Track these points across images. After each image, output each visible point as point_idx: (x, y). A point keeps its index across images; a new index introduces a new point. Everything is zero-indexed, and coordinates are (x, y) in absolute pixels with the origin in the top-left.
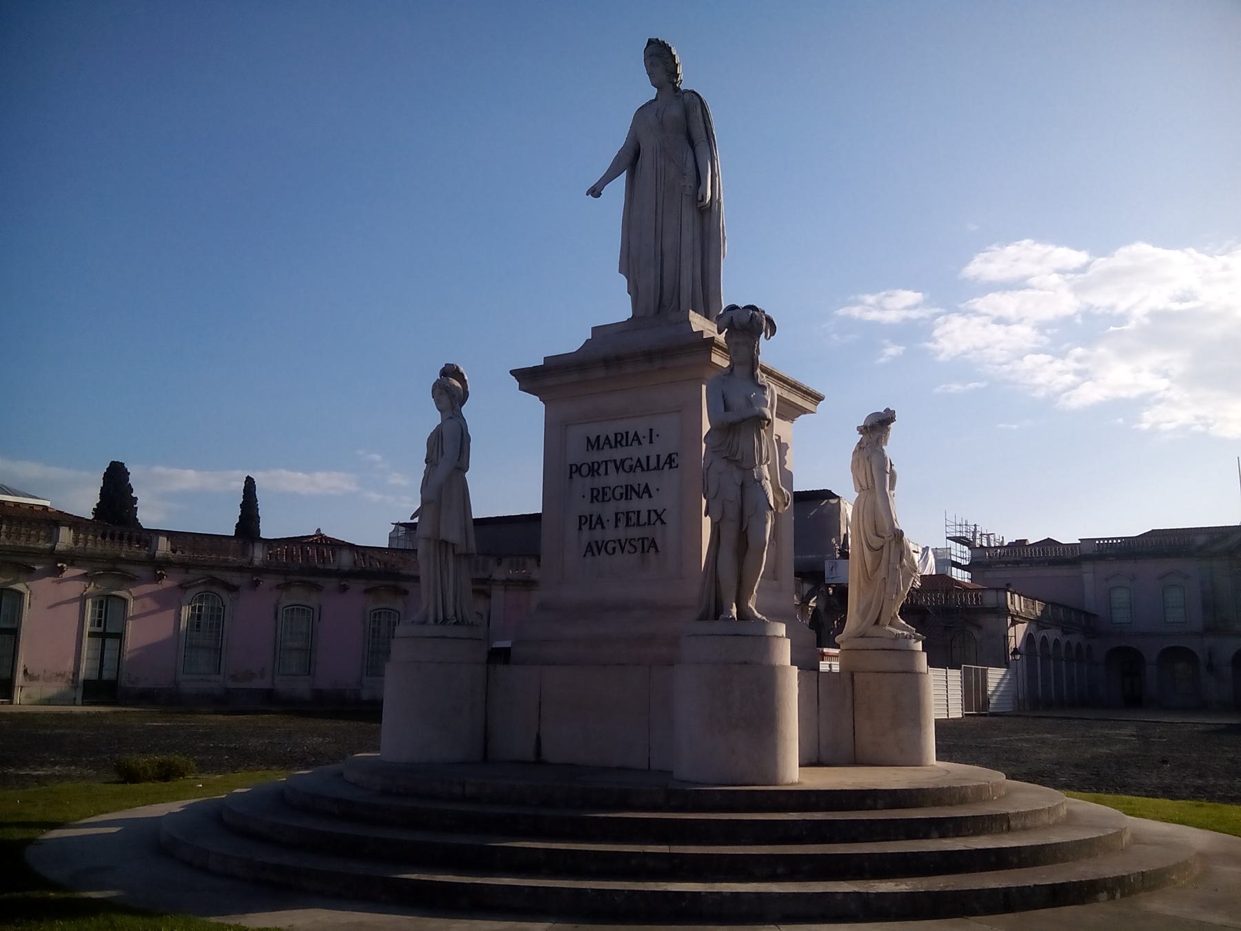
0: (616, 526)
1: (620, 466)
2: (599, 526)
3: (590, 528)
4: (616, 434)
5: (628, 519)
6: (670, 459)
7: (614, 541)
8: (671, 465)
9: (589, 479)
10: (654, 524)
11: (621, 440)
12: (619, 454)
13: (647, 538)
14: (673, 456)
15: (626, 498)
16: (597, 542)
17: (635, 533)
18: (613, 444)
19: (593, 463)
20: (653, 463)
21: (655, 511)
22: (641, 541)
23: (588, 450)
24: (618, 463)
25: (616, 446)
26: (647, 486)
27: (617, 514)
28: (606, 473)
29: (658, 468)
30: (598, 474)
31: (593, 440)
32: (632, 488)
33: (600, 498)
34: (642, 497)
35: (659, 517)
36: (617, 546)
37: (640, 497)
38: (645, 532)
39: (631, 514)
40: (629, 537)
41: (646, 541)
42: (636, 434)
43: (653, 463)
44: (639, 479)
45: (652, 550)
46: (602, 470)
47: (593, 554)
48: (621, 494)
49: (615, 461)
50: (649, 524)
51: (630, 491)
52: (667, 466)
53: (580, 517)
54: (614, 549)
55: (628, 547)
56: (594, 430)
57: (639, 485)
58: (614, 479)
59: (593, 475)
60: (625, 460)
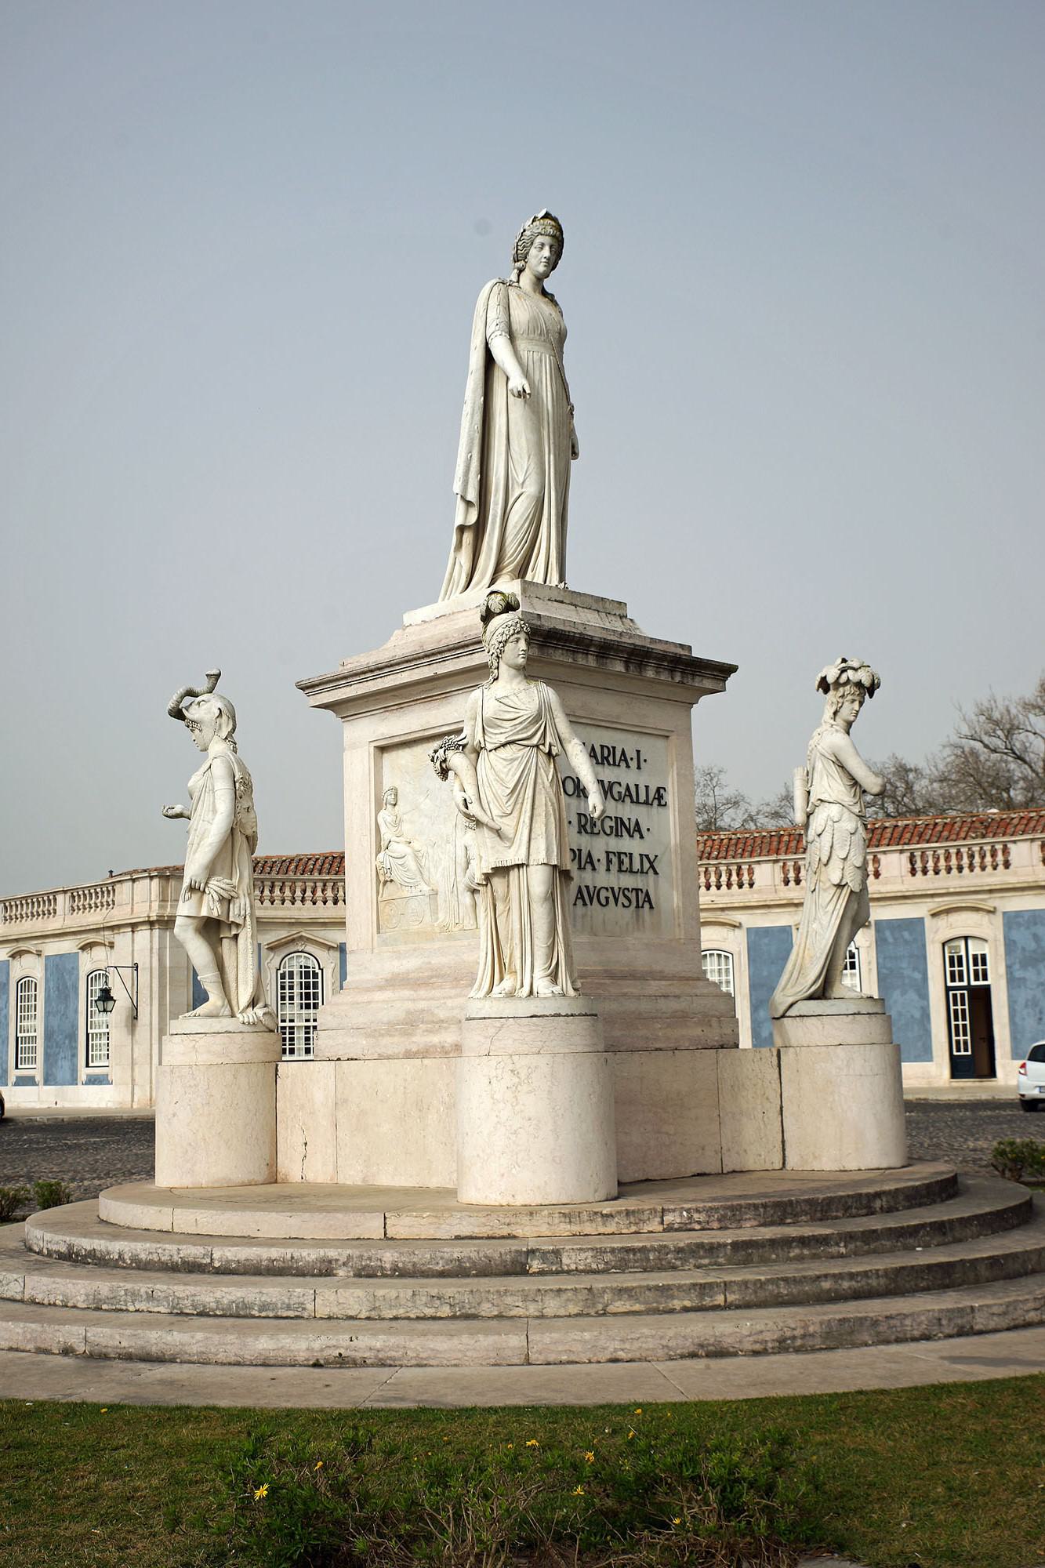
0: (608, 870)
2: (589, 866)
4: (602, 747)
5: (621, 862)
6: (659, 795)
7: (607, 889)
8: (659, 802)
13: (641, 890)
14: (662, 791)
15: (617, 835)
16: (587, 887)
17: (628, 881)
18: (600, 761)
21: (647, 856)
24: (606, 785)
26: (637, 823)
27: (608, 853)
29: (646, 803)
32: (623, 823)
36: (610, 894)
37: (631, 836)
39: (623, 857)
40: (623, 886)
43: (642, 798)
45: (647, 905)
47: (585, 904)
48: (611, 827)
52: (656, 802)
54: (607, 898)
55: (622, 899)
59: (579, 796)
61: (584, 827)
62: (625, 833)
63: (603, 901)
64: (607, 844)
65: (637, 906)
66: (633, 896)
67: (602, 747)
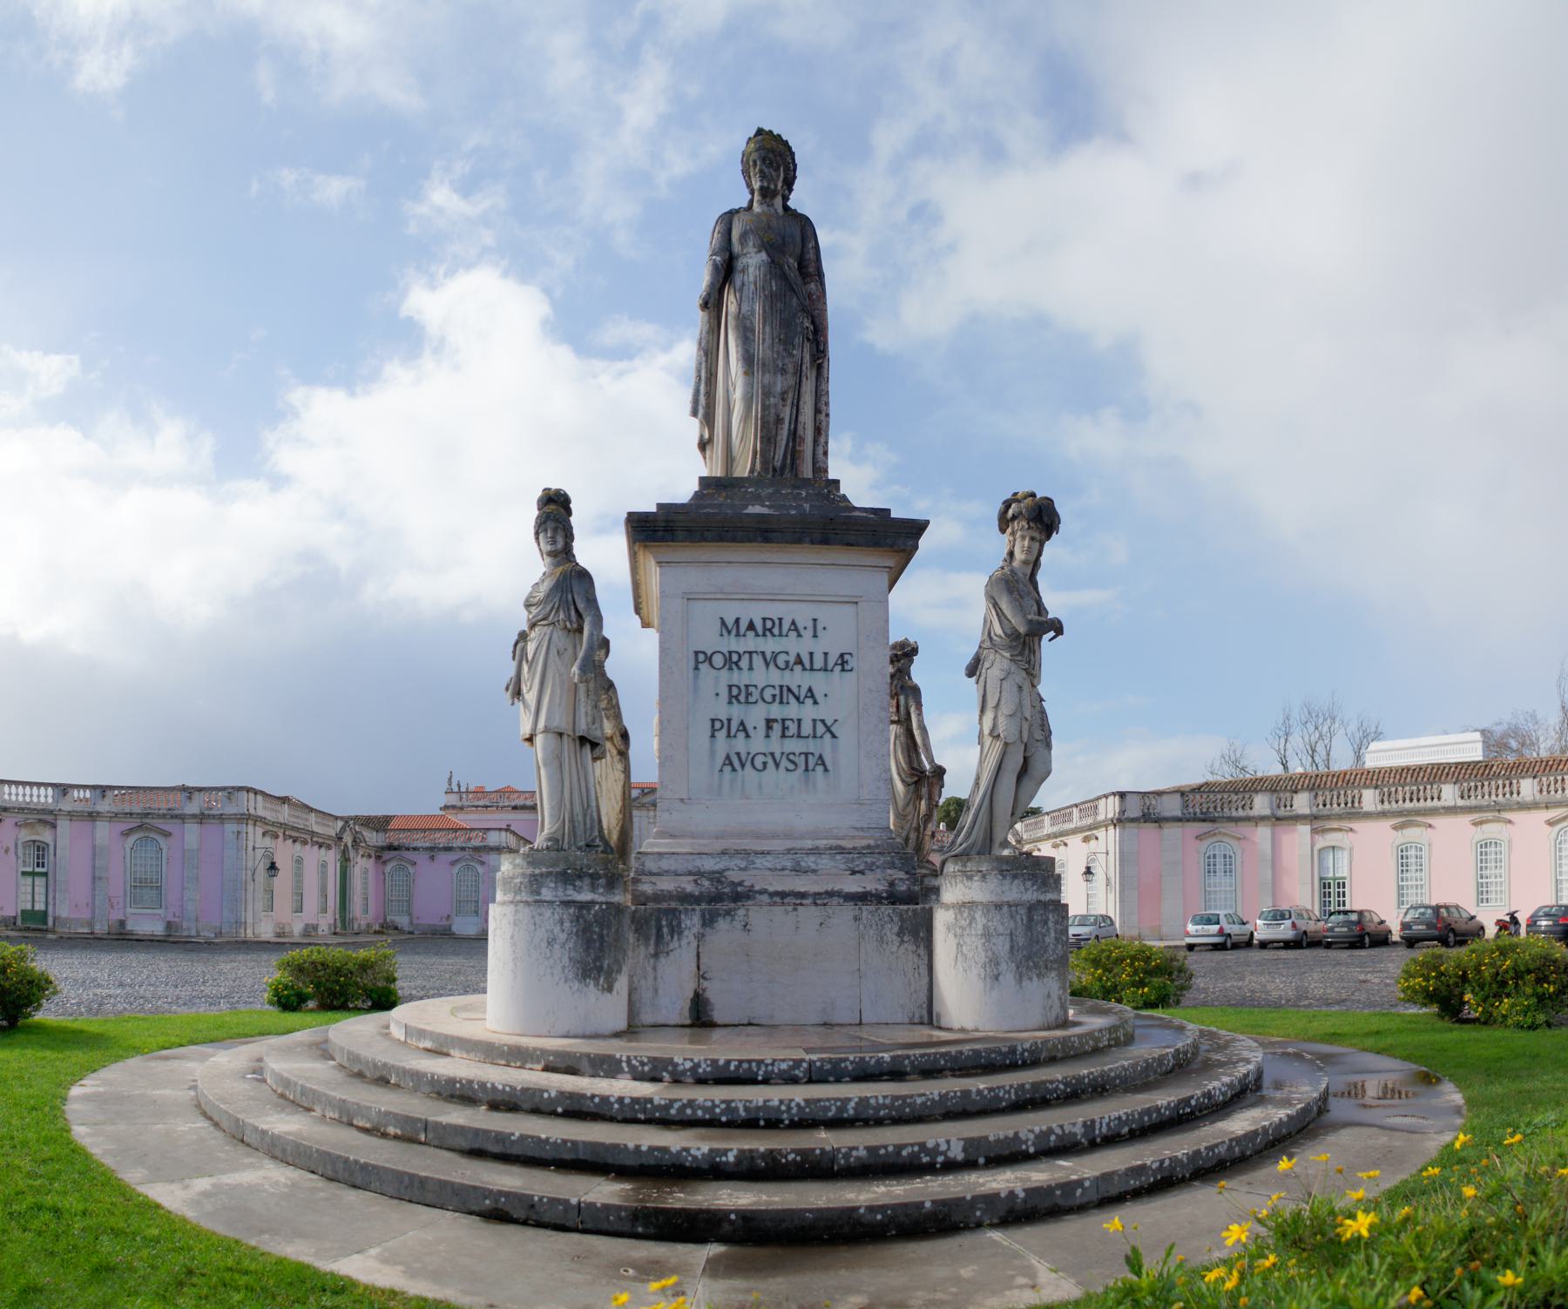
1: (770, 661)
2: (741, 735)
3: (729, 736)
4: (764, 619)
5: (785, 728)
6: (842, 661)
7: (765, 754)
9: (724, 672)
10: (821, 737)
11: (770, 628)
12: (770, 645)
13: (812, 754)
15: (781, 702)
16: (738, 754)
18: (760, 633)
19: (730, 653)
20: (818, 663)
22: (803, 757)
23: (722, 635)
25: (764, 635)
26: (810, 690)
28: (751, 668)
30: (740, 668)
31: (730, 623)
32: (789, 690)
33: (742, 698)
34: (803, 703)
35: (828, 729)
38: (811, 746)
40: (787, 750)
41: (810, 757)
42: (793, 623)
43: (818, 663)
44: (797, 679)
45: (820, 769)
46: (744, 663)
47: (734, 770)
48: (774, 696)
49: (763, 653)
50: (815, 737)
51: (785, 694)
52: (839, 668)
53: (713, 721)
54: (765, 764)
55: (784, 763)
56: (731, 611)
57: (799, 686)
58: (761, 676)
60: (779, 653)
61: (736, 697)
62: (792, 700)
63: (760, 766)
64: (768, 712)
65: (807, 769)
66: (801, 761)
67: (764, 619)
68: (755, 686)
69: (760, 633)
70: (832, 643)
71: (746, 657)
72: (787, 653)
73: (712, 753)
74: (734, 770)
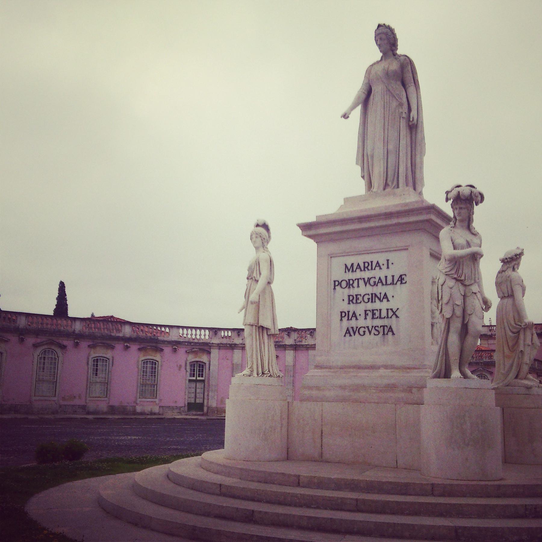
2: (354, 319)
3: (348, 319)
4: (364, 263)
5: (374, 314)
6: (401, 279)
7: (364, 327)
10: (391, 317)
11: (368, 266)
12: (366, 275)
13: (387, 326)
15: (372, 302)
18: (362, 269)
19: (349, 280)
20: (390, 280)
22: (382, 328)
26: (385, 294)
28: (358, 286)
31: (349, 266)
32: (376, 295)
41: (386, 327)
43: (390, 280)
45: (390, 333)
46: (355, 284)
47: (351, 335)
48: (369, 299)
49: (364, 279)
51: (373, 297)
52: (399, 282)
53: (341, 312)
54: (364, 332)
55: (373, 331)
56: (349, 261)
57: (380, 293)
58: (363, 290)
60: (371, 278)
63: (362, 333)
64: (366, 307)
65: (384, 334)
68: (361, 295)
69: (362, 269)
70: (395, 271)
71: (356, 282)
72: (375, 278)
73: (341, 327)
74: (351, 335)
